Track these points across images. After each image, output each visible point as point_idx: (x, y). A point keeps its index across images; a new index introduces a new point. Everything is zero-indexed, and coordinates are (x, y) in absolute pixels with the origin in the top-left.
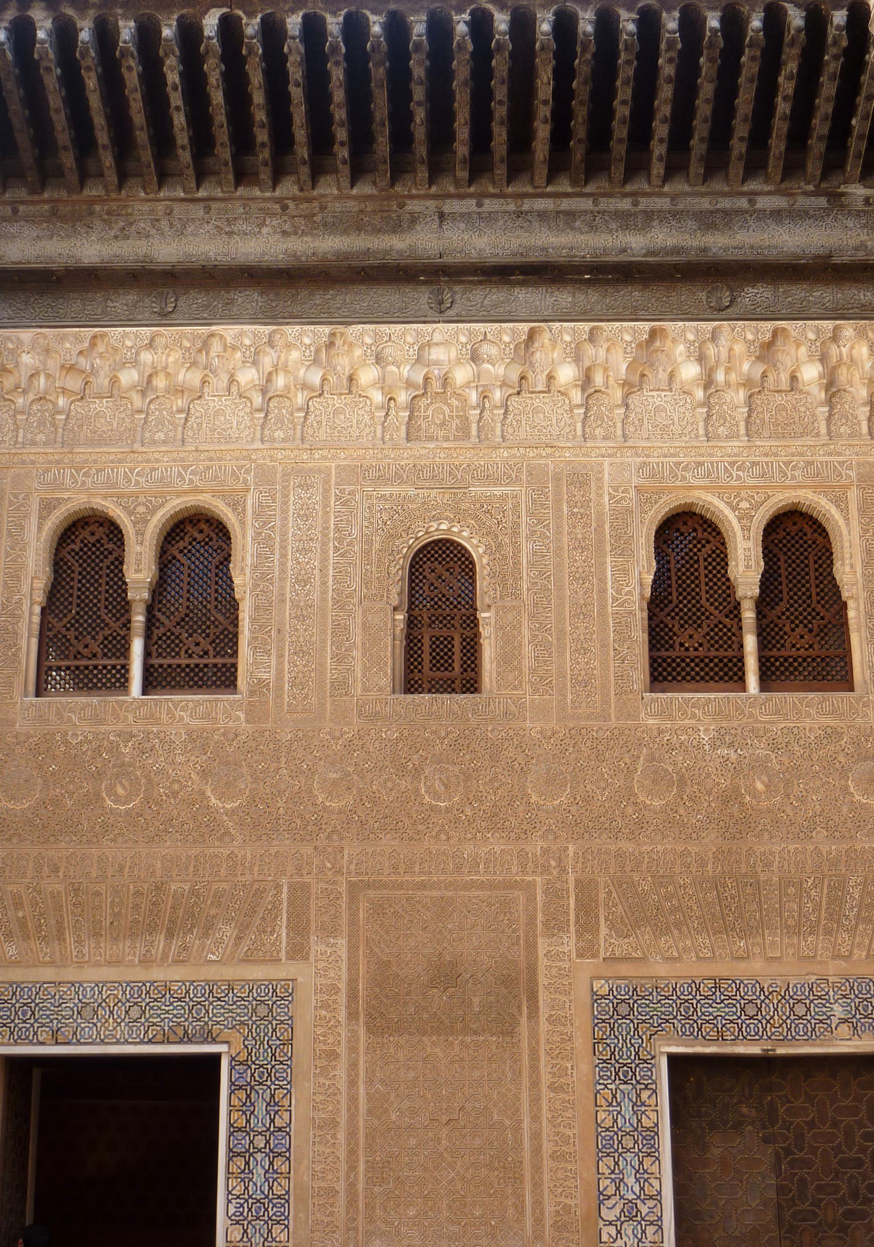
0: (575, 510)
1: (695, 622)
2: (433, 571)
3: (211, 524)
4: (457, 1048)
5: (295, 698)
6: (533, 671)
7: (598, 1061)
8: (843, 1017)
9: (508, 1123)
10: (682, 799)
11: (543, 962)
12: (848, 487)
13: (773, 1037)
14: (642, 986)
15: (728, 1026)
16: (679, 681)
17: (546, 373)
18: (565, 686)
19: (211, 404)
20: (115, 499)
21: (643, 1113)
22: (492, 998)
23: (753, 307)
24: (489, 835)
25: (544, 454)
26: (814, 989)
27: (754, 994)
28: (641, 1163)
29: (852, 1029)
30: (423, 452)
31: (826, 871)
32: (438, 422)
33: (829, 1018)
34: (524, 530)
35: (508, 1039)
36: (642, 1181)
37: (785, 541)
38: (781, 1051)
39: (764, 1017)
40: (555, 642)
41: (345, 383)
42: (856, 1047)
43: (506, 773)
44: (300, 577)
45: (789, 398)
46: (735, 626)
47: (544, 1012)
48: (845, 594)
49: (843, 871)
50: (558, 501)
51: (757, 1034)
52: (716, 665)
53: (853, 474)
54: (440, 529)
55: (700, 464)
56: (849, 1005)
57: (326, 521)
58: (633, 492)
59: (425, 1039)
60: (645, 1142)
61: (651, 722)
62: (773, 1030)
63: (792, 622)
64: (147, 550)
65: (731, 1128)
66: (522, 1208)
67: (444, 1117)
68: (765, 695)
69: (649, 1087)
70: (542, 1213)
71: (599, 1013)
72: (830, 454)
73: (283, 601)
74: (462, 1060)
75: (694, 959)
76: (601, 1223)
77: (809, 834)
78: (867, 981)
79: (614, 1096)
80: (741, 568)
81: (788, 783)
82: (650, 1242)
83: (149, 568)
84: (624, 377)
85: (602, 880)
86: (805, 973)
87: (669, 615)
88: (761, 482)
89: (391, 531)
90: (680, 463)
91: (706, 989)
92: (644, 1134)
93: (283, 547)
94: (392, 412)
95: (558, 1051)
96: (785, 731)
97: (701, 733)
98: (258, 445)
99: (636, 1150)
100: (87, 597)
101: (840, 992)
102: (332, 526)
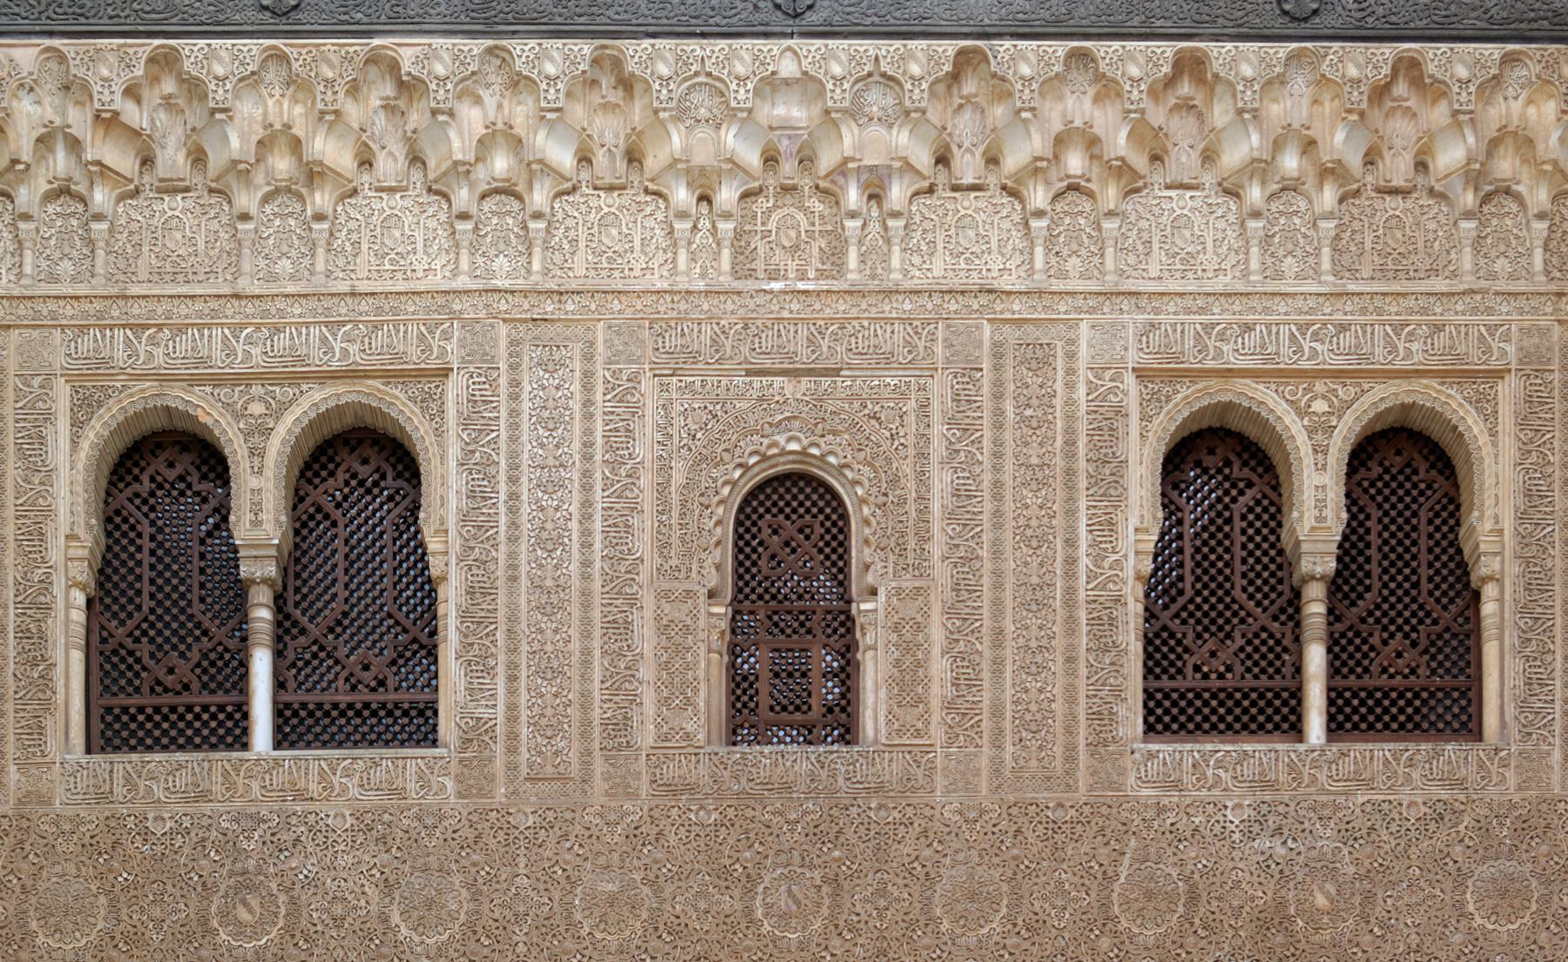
0: (1029, 412)
1: (1221, 629)
3: (382, 449)
5: (540, 753)
6: (949, 706)
12: (1498, 374)
16: (1190, 732)
17: (982, 148)
19: (376, 205)
20: (208, 389)
23: (1359, 15)
25: (976, 307)
32: (787, 244)
34: (937, 449)
37: (1380, 484)
40: (987, 653)
41: (621, 165)
43: (900, 881)
44: (545, 535)
45: (1409, 203)
50: (998, 396)
52: (1254, 704)
53: (1511, 349)
55: (1248, 328)
57: (588, 432)
58: (1130, 380)
63: (1385, 629)
64: (271, 485)
72: (1475, 310)
73: (514, 579)
80: (1308, 522)
83: (277, 521)
84: (1122, 153)
89: (704, 451)
90: (1214, 325)
93: (513, 480)
94: (705, 224)
98: (463, 282)
100: (168, 581)
102: (599, 441)
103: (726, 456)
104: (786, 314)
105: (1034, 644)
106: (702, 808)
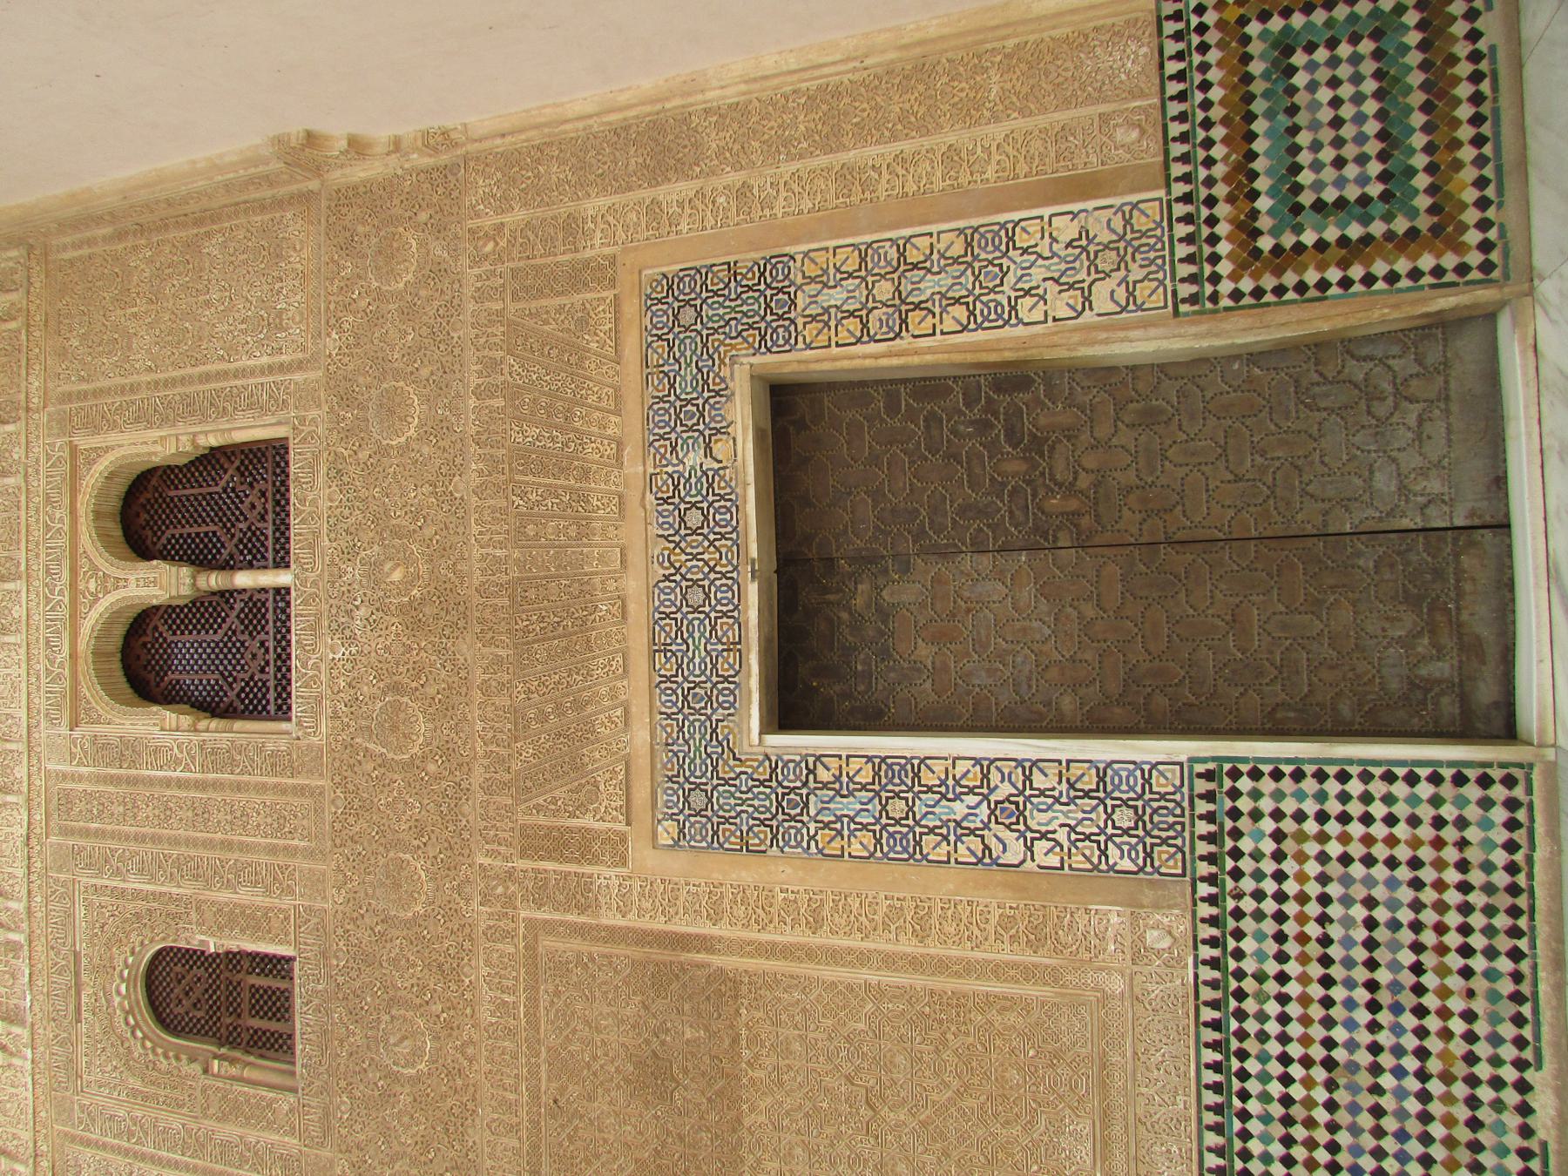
0: (95, 812)
2: (180, 1001)
4: (759, 1074)
6: (268, 892)
7: (775, 847)
8: (702, 451)
9: (869, 1006)
10: (417, 689)
11: (632, 921)
12: (74, 450)
13: (735, 562)
14: (664, 766)
15: (720, 633)
18: (286, 848)
21: (851, 779)
22: (687, 1007)
24: (467, 981)
25: (39, 848)
26: (665, 496)
27: (673, 590)
28: (930, 789)
29: (719, 436)
30: (37, 1008)
31: (504, 477)
32: (11, 981)
33: (705, 473)
34: (116, 883)
35: (744, 989)
36: (958, 790)
38: (754, 552)
39: (706, 577)
40: (236, 856)
42: (745, 429)
46: (241, 597)
47: (707, 929)
48: (189, 448)
49: (504, 452)
50: (86, 833)
51: (730, 588)
54: (125, 993)
55: (48, 642)
56: (685, 441)
58: (77, 733)
59: (747, 1122)
60: (897, 781)
61: (324, 729)
62: (724, 561)
65: (885, 622)
66: (1006, 998)
67: (862, 1111)
68: (293, 566)
69: (811, 766)
70: (1014, 965)
71: (704, 839)
72: (37, 472)
74: (777, 1068)
75: (625, 683)
76: (1029, 865)
77: (457, 502)
78: (651, 413)
79: (827, 825)
81: (396, 533)
82: (1060, 782)
85: (523, 819)
86: (642, 510)
87: (230, 685)
88: (66, 563)
91: (668, 666)
92: (884, 781)
95: (760, 911)
96: (333, 535)
97: (337, 657)
99: (910, 795)
101: (668, 456)
103: (126, 1045)
104: (45, 990)
105: (229, 817)
106: (339, 1108)
